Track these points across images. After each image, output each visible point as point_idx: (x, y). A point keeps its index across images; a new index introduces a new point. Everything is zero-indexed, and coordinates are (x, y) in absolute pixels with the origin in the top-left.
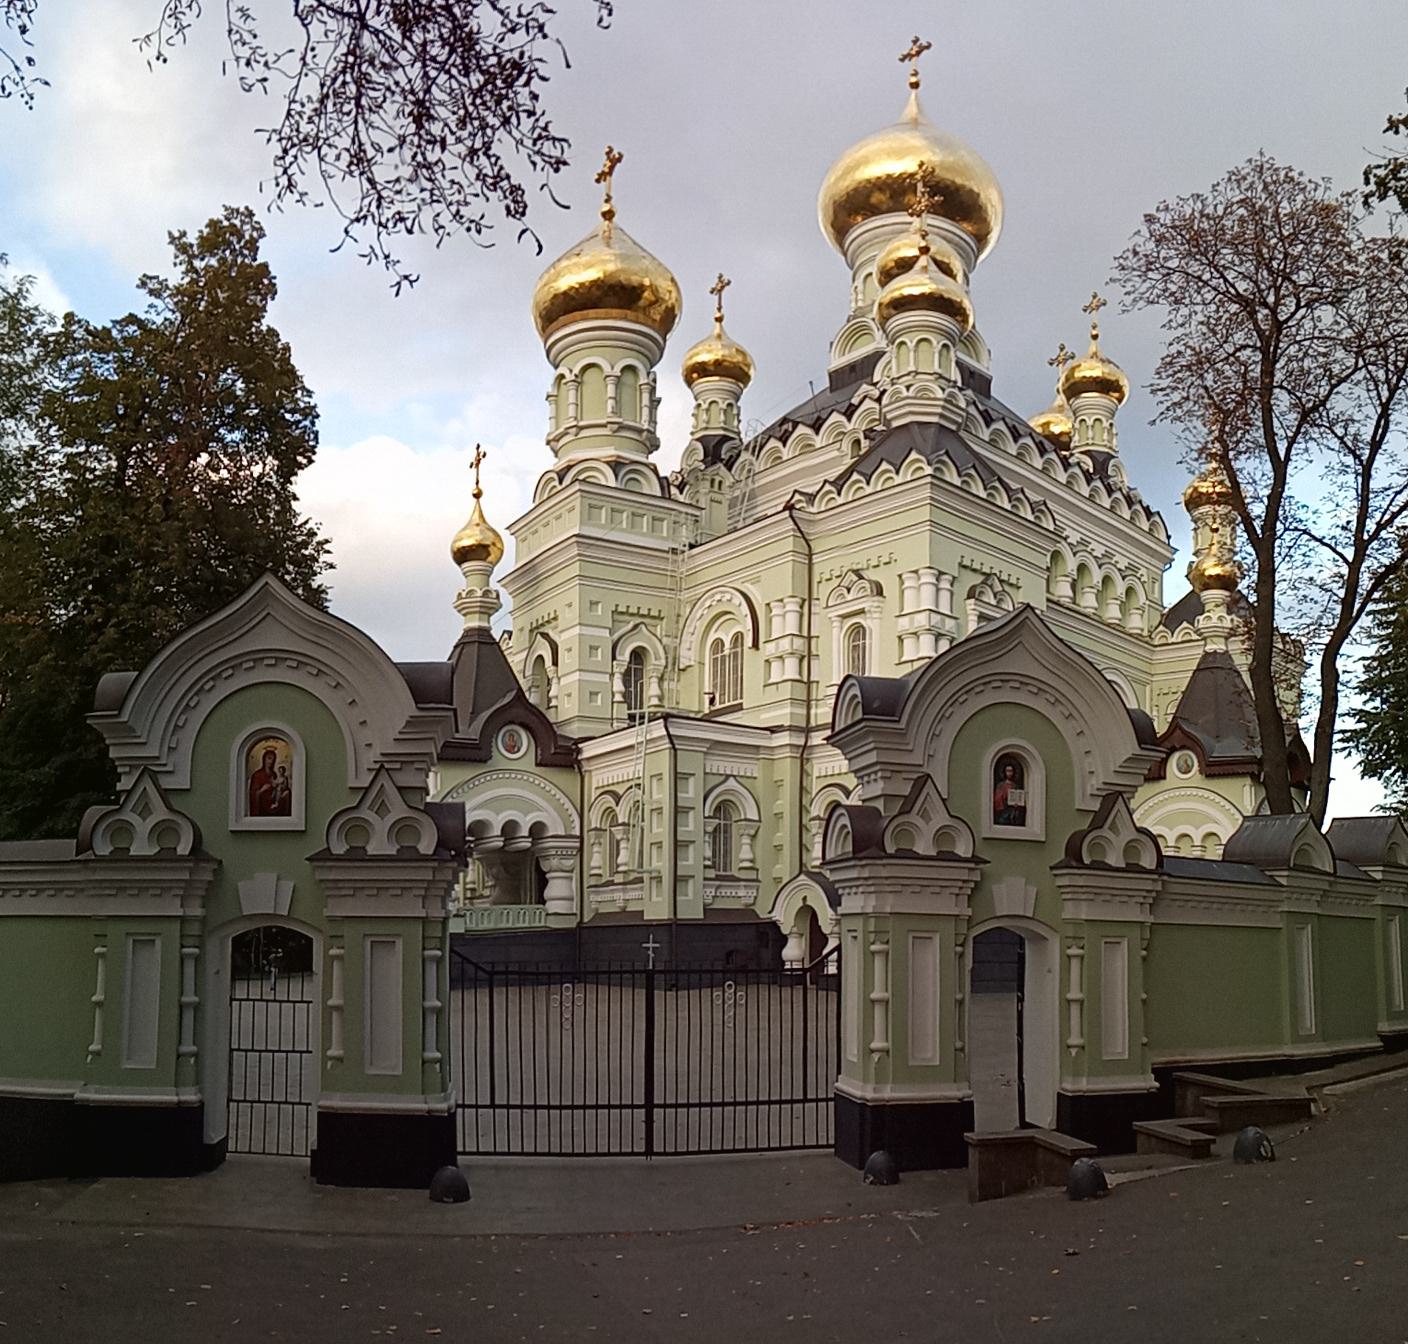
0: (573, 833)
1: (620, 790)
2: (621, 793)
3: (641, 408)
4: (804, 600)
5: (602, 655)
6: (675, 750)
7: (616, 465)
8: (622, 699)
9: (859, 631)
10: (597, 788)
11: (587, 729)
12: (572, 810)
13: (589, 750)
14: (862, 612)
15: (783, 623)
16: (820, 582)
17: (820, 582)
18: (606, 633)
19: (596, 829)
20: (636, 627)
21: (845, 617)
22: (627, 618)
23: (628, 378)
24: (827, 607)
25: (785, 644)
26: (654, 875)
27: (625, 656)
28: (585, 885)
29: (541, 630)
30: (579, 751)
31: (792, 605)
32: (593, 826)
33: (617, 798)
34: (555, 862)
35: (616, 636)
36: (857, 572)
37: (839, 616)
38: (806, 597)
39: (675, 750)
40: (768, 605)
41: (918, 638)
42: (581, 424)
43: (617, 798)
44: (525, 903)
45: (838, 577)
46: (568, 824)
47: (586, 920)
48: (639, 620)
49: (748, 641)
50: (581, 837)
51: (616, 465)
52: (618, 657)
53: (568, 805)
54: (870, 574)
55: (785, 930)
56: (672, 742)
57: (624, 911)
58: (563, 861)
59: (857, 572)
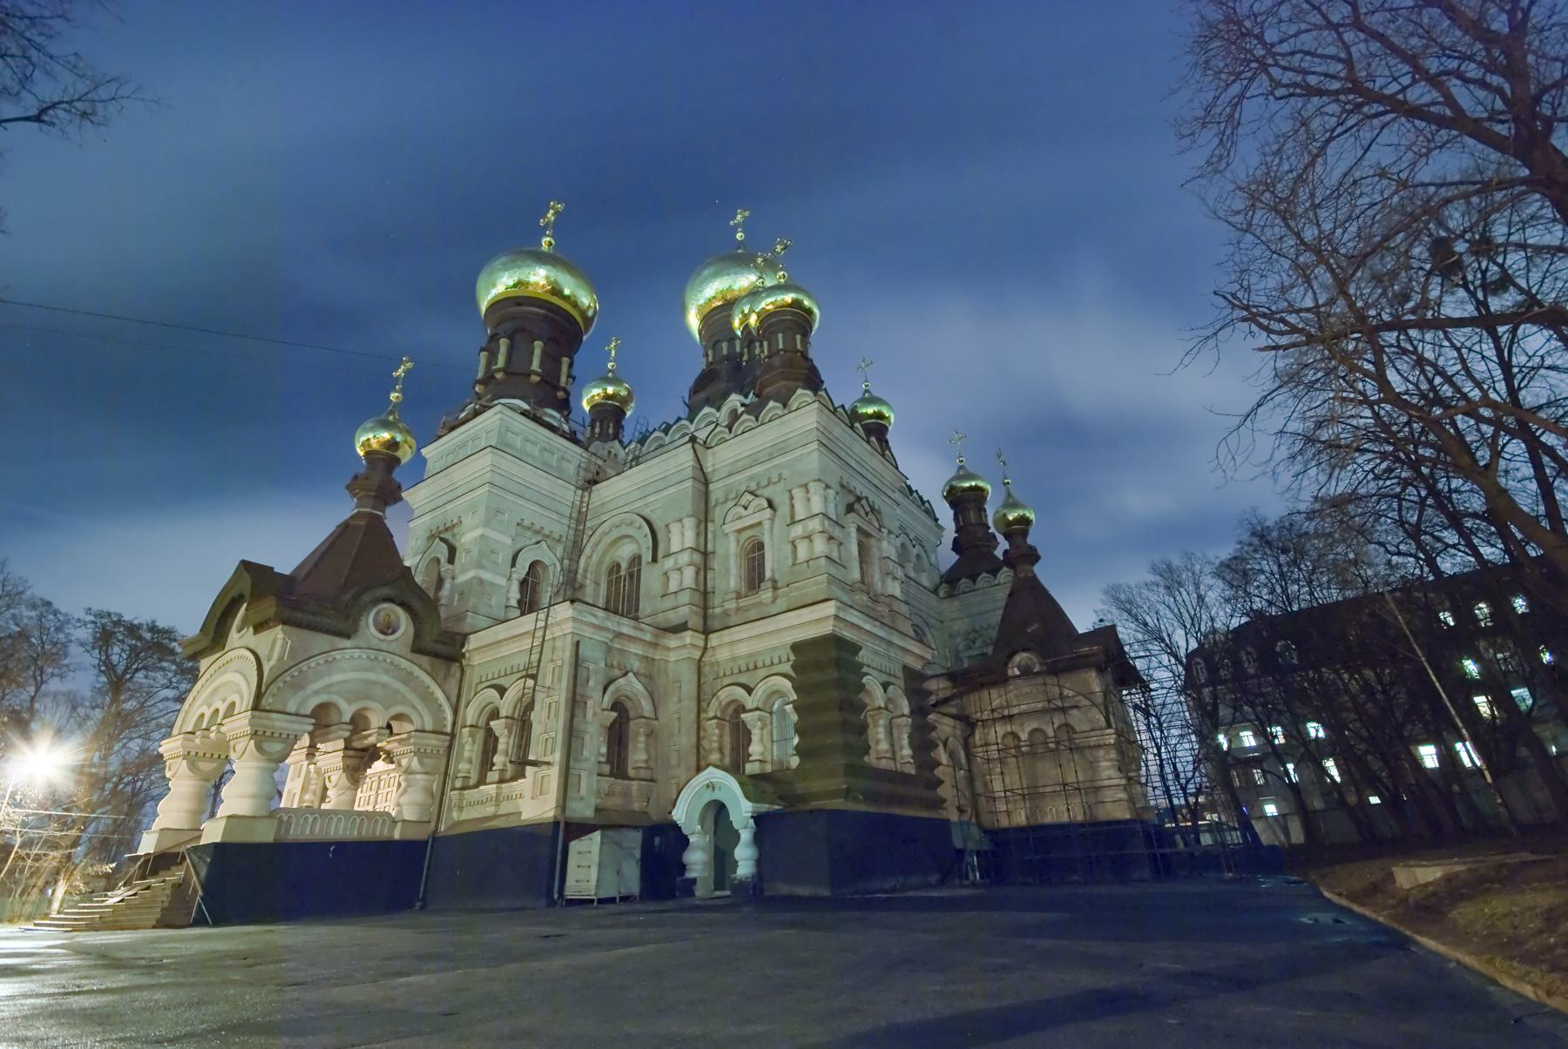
0: (444, 730)
5: (504, 557)
8: (516, 605)
15: (681, 537)
17: (715, 506)
18: (509, 541)
20: (538, 543)
21: (739, 531)
31: (689, 523)
33: (502, 691)
36: (752, 493)
38: (702, 518)
41: (811, 541)
43: (502, 691)
47: (442, 828)
49: (647, 556)
54: (767, 492)
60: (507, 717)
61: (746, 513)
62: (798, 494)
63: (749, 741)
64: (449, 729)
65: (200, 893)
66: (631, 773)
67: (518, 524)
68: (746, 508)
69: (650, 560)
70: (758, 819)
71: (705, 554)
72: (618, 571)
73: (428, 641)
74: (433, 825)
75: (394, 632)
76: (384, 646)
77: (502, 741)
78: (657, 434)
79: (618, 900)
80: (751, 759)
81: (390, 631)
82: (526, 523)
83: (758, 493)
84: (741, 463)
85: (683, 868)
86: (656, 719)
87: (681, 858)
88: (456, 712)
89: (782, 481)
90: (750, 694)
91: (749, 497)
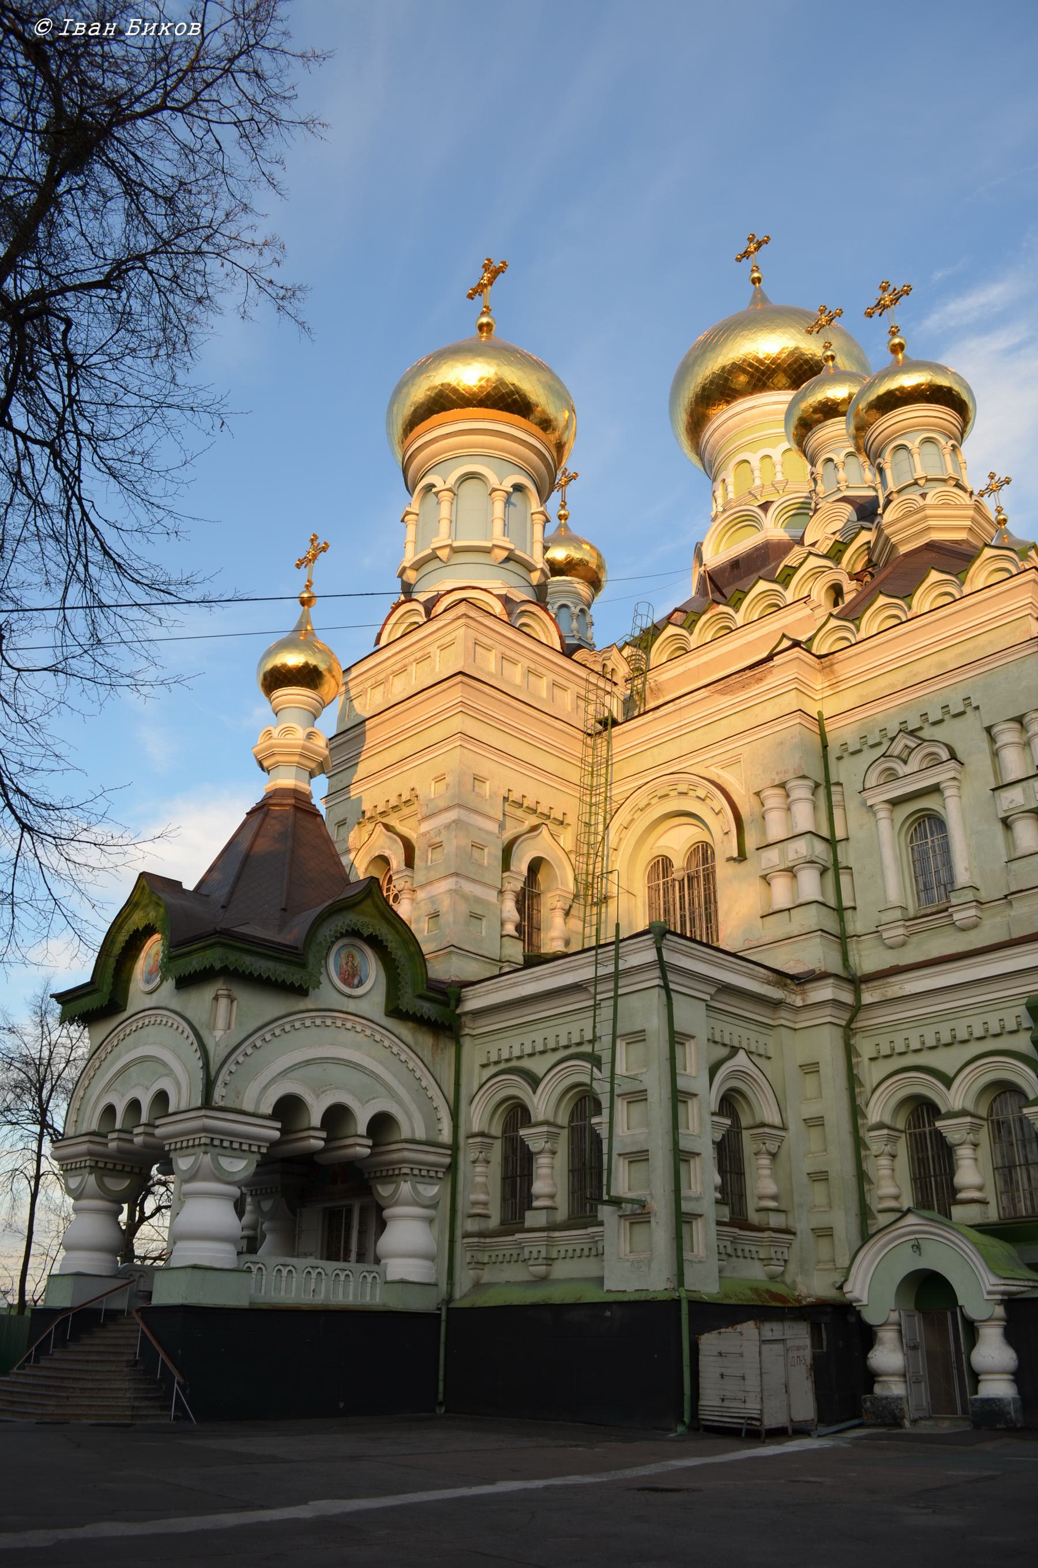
1: (537, 1066)
2: (540, 1073)
3: (532, 543)
4: (817, 785)
5: (491, 856)
6: (668, 991)
7: (506, 600)
8: (516, 934)
9: (935, 822)
10: (483, 1066)
11: (470, 970)
12: (439, 1102)
13: (474, 1001)
14: (935, 789)
16: (840, 758)
17: (840, 758)
18: (493, 827)
19: (482, 1134)
21: (895, 803)
22: (519, 813)
23: (516, 498)
24: (864, 790)
25: (801, 848)
26: (628, 1208)
27: (521, 865)
28: (459, 1233)
29: (384, 820)
30: (459, 1001)
32: (476, 1128)
34: (405, 1188)
35: (508, 835)
36: (912, 733)
37: (886, 801)
38: (821, 780)
39: (668, 991)
40: (758, 794)
42: (456, 544)
43: (534, 1081)
44: (346, 1259)
45: (872, 746)
46: (432, 1120)
48: (533, 820)
49: (726, 846)
50: (454, 1148)
51: (506, 600)
52: (512, 868)
53: (434, 1091)
55: (871, 1317)
56: (664, 977)
57: (544, 1279)
58: (421, 1188)
59: (912, 733)
60: (546, 1123)
61: (902, 769)
62: (1008, 735)
63: (950, 1169)
64: (446, 1137)
65: (178, 1377)
66: (754, 1217)
67: (506, 799)
68: (905, 762)
69: (735, 855)
70: (1012, 1304)
71: (832, 842)
72: (666, 872)
73: (409, 1002)
74: (444, 1287)
75: (361, 983)
76: (351, 1006)
77: (543, 1166)
78: (671, 630)
79: (790, 1431)
80: (961, 1196)
81: (356, 981)
82: (515, 796)
83: (925, 734)
84: (882, 682)
85: (871, 1377)
86: (784, 1128)
87: (865, 1358)
88: (455, 1115)
89: (970, 713)
90: (949, 1087)
91: (903, 741)
